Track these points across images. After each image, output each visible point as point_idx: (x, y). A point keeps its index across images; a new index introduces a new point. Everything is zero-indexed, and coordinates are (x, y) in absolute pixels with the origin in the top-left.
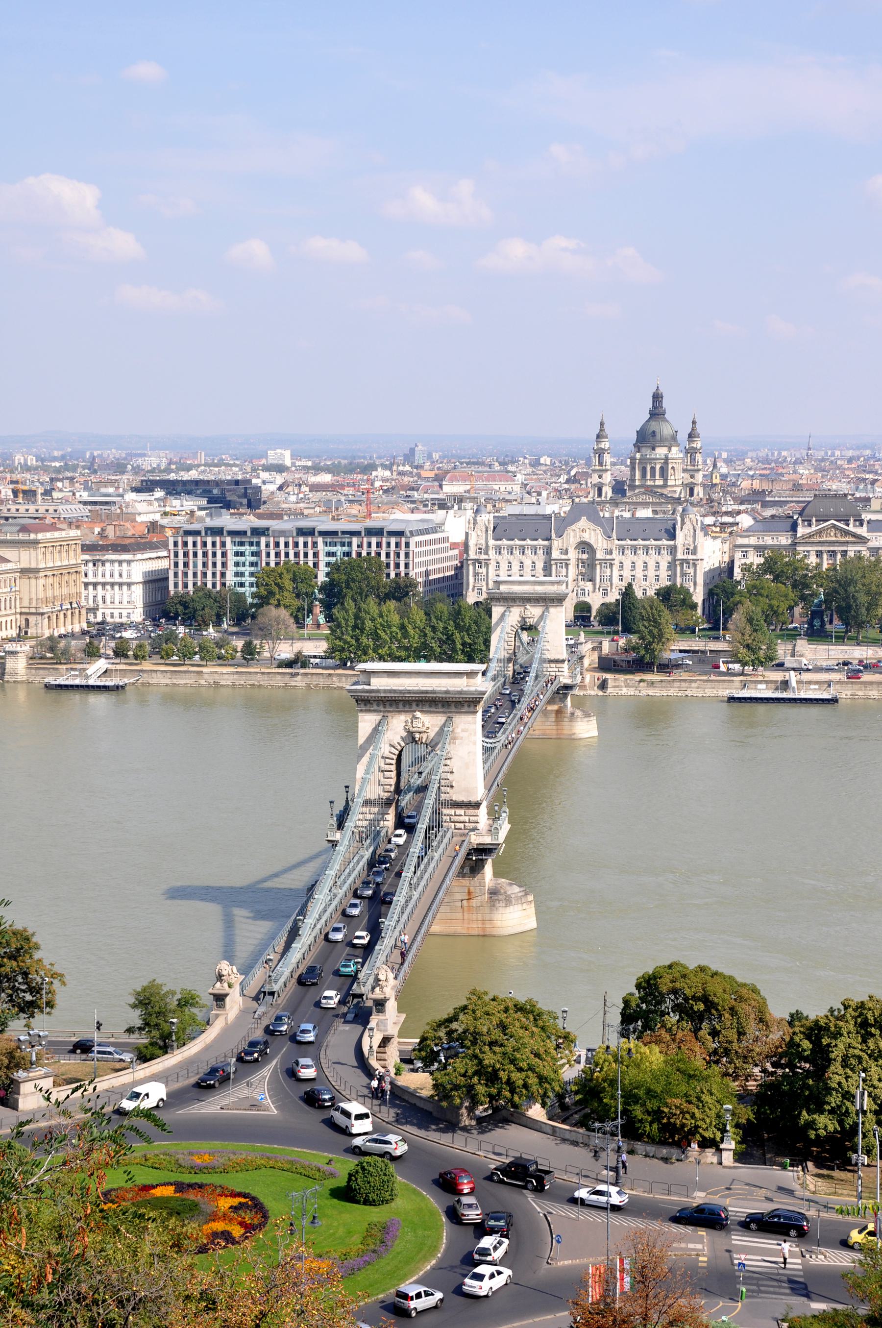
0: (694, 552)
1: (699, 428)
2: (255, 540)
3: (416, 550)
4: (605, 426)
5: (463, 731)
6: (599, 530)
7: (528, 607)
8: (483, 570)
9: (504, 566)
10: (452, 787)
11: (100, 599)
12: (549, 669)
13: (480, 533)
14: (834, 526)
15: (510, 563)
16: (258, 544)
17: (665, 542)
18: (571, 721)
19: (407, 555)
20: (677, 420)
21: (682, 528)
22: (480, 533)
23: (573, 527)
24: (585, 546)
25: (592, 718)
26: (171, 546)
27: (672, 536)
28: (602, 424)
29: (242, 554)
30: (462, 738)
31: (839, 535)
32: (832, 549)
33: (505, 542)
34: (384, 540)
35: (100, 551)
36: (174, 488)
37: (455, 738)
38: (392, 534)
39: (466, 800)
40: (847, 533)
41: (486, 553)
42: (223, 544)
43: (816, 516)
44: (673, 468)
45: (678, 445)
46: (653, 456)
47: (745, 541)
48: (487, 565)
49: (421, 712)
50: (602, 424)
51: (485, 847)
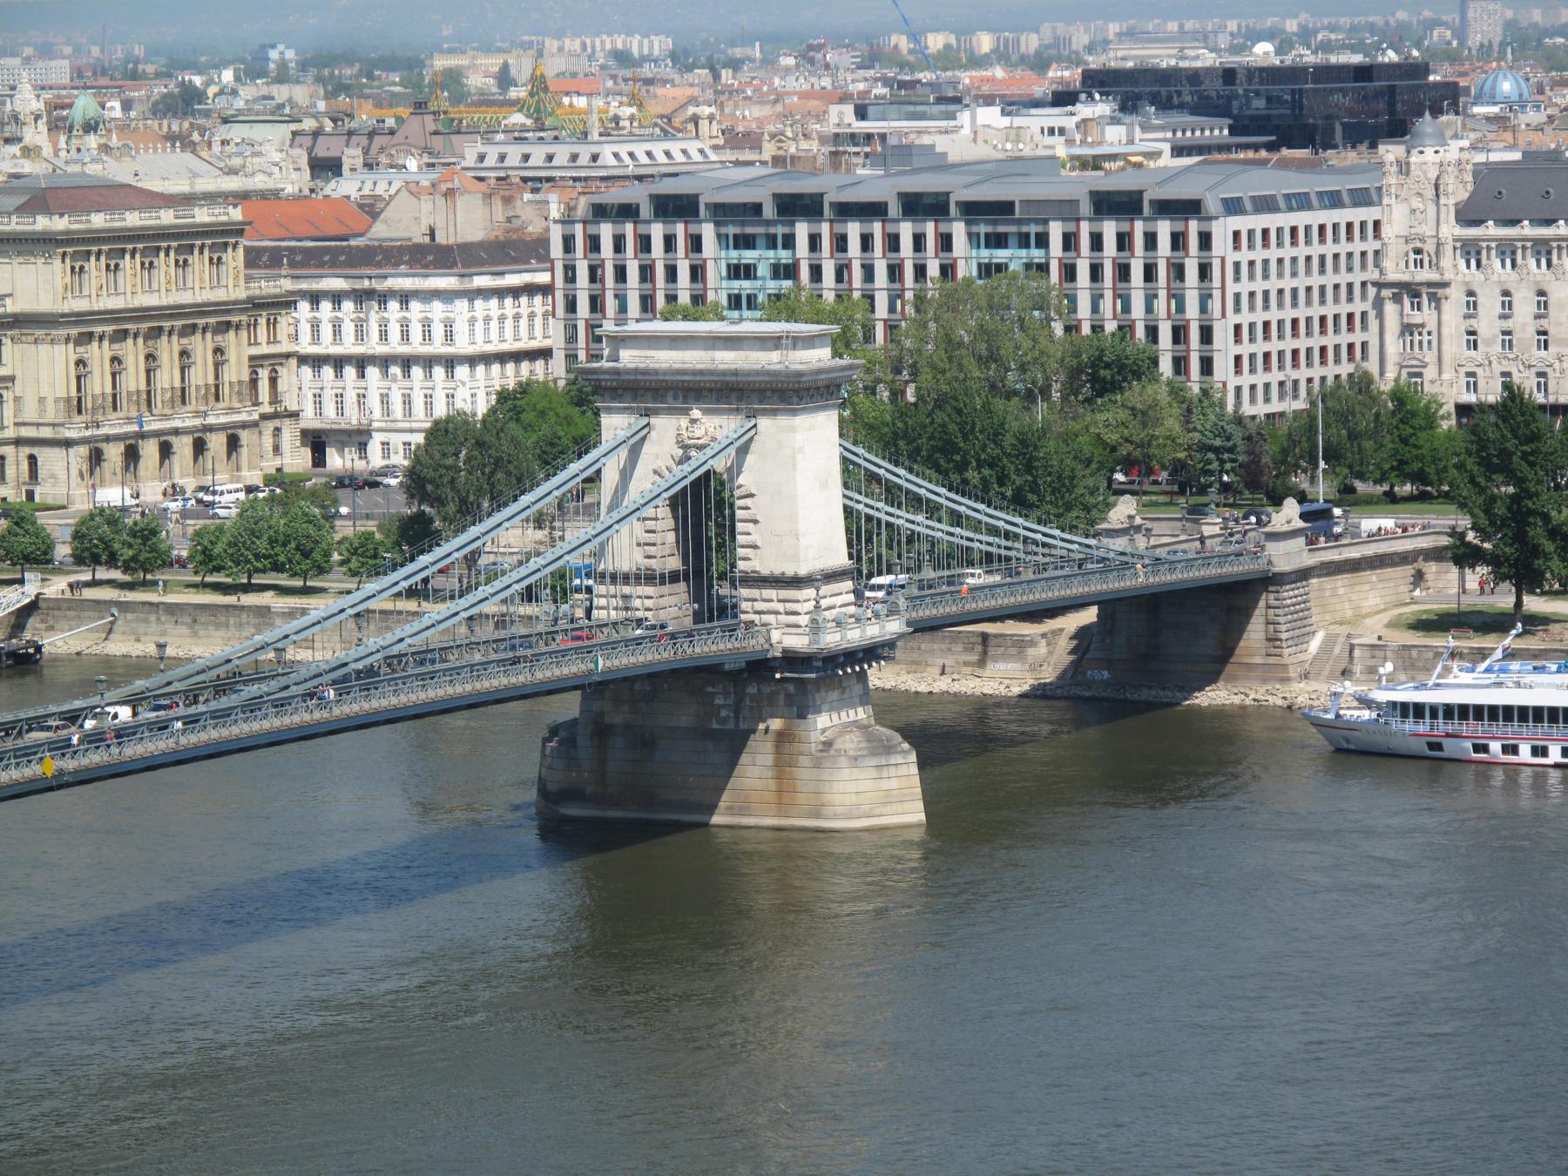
2: (780, 230)
7: (696, 413)
8: (1426, 315)
9: (1490, 304)
11: (374, 402)
12: (759, 606)
13: (1416, 203)
15: (1506, 293)
16: (789, 242)
18: (817, 765)
19: (1204, 271)
25: (899, 759)
26: (556, 250)
29: (747, 272)
33: (1491, 230)
34: (1139, 227)
35: (379, 265)
36: (1135, 90)
41: (1435, 265)
42: (696, 243)
48: (1436, 300)
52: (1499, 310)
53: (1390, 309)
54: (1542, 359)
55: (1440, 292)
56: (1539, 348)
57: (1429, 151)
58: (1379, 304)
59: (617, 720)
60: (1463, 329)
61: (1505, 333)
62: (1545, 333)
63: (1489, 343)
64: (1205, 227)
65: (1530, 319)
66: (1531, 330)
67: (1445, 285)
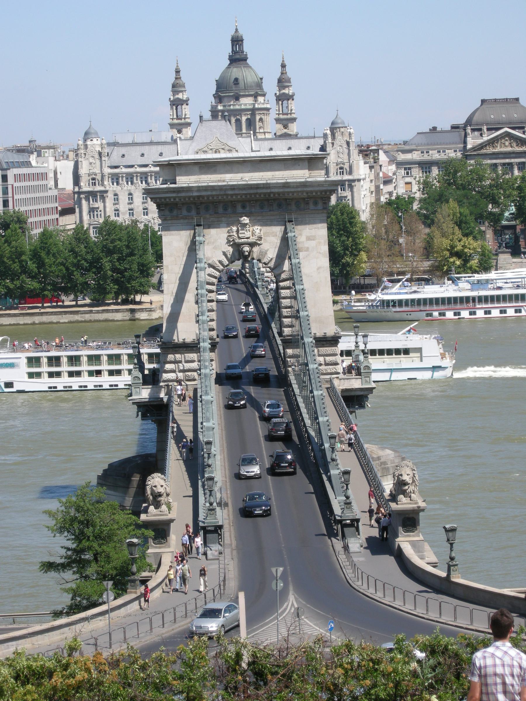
0: (350, 173)
1: (290, 72)
3: (16, 185)
4: (181, 74)
5: (309, 239)
8: (99, 204)
9: (124, 199)
13: (91, 160)
14: (508, 134)
20: (262, 65)
21: (333, 144)
22: (91, 160)
28: (178, 72)
30: (307, 249)
31: (514, 144)
32: (507, 161)
43: (487, 124)
44: (261, 120)
45: (264, 95)
46: (237, 107)
47: (408, 157)
48: (103, 199)
50: (178, 72)
51: (353, 394)
52: (127, 201)
53: (84, 203)
54: (146, 220)
55: (105, 195)
56: (144, 215)
57: (95, 140)
58: (80, 199)
60: (113, 209)
61: (129, 210)
62: (147, 209)
63: (124, 214)
64: (4, 173)
65: (140, 204)
66: (141, 208)
67: (106, 192)
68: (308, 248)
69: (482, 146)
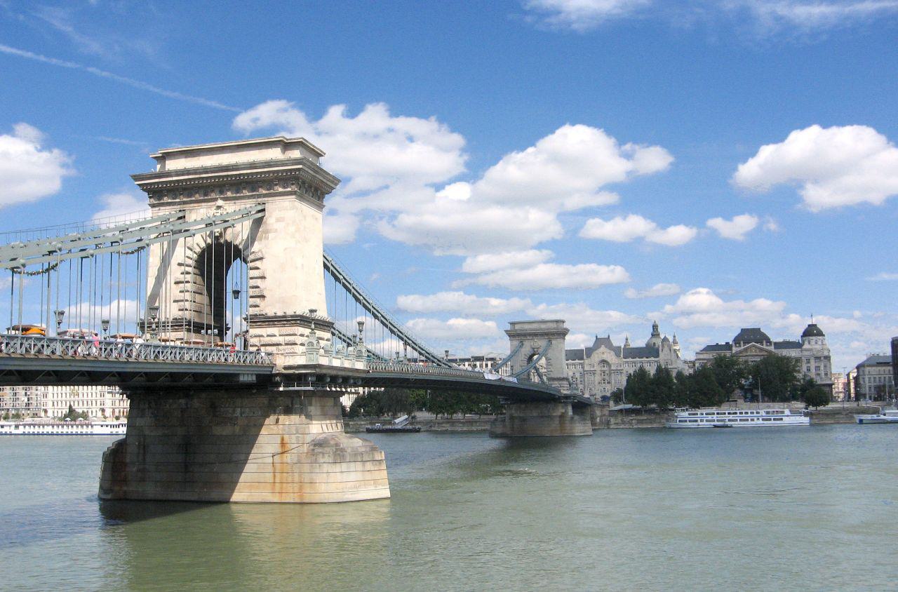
5: (278, 220)
6: (613, 353)
10: (263, 297)
14: (754, 346)
17: (653, 359)
23: (597, 351)
24: (604, 362)
27: (658, 356)
28: (627, 339)
31: (758, 351)
37: (267, 232)
38: (488, 360)
39: (280, 313)
40: (762, 350)
49: (226, 199)
50: (627, 339)
59: (516, 415)
68: (276, 229)
69: (741, 352)
